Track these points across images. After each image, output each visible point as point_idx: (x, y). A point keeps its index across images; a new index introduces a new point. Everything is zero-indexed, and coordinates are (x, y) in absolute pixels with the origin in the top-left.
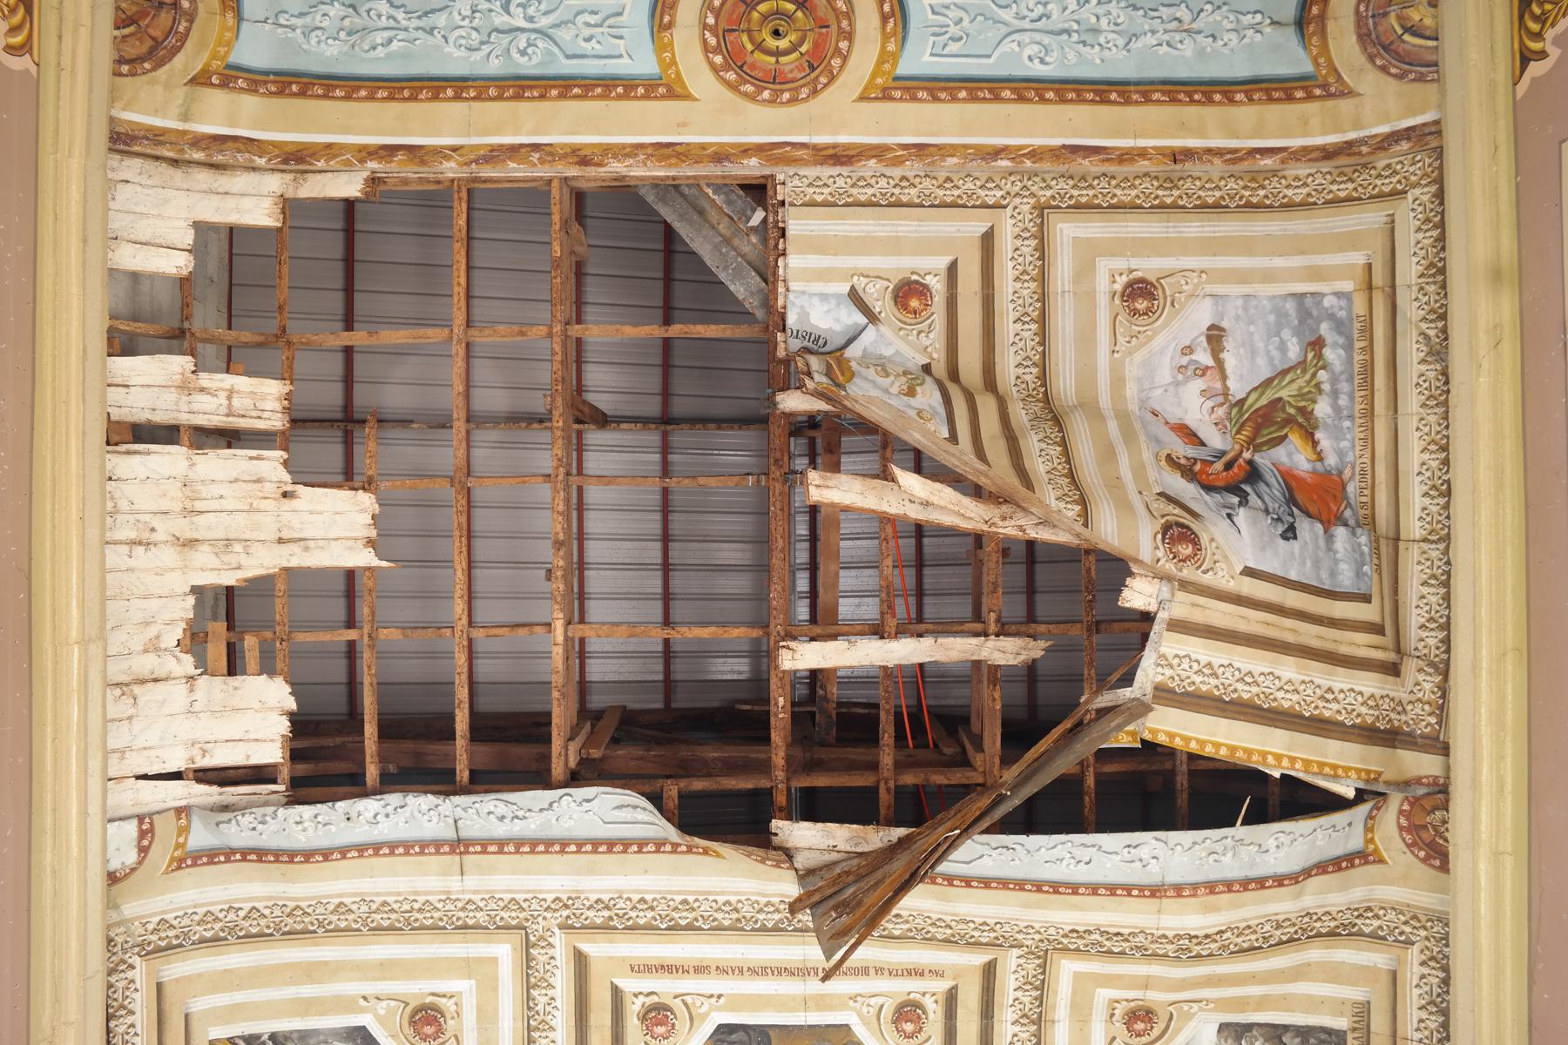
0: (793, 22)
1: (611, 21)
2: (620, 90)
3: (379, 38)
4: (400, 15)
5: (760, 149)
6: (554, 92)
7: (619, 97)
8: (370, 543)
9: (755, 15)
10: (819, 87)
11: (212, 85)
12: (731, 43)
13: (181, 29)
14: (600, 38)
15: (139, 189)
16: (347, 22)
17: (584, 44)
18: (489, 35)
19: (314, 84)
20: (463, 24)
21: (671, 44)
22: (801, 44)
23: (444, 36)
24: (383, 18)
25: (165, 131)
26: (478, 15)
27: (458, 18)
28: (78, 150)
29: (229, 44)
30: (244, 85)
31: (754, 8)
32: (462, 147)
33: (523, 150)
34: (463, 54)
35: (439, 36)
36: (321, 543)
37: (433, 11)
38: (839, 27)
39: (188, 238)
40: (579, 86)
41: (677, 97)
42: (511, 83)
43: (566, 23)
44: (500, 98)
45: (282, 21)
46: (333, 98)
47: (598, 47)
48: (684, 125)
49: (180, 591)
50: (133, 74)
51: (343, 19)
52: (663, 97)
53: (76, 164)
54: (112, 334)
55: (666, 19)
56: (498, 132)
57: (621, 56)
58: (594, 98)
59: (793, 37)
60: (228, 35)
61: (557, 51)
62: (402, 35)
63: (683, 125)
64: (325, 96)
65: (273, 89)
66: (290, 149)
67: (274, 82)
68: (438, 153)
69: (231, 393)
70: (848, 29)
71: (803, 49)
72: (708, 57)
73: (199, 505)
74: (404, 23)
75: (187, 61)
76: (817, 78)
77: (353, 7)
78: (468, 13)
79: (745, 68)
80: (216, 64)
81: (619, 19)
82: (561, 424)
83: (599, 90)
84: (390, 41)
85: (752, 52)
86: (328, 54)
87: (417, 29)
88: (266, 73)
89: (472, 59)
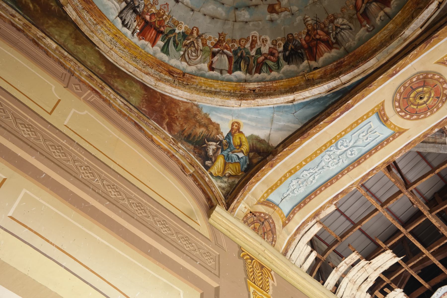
0: (424, 92)
1: (370, 130)
2: (385, 143)
3: (311, 179)
4: (311, 171)
5: (436, 126)
6: (368, 156)
7: (386, 144)
8: (395, 257)
9: (411, 99)
10: (444, 101)
11: (287, 223)
12: (409, 110)
13: (271, 221)
14: (370, 136)
15: (294, 253)
16: (299, 182)
17: (367, 141)
18: (339, 157)
19: (306, 200)
20: (329, 160)
21: (391, 123)
22: (431, 94)
23: (327, 167)
24: (308, 175)
25: (289, 241)
26: (332, 156)
27: (327, 160)
28: (288, 270)
29: (282, 213)
30: (292, 215)
31: (409, 97)
32: (354, 183)
33: (371, 172)
34: (335, 167)
35: (326, 167)
36: (384, 264)
37: (319, 164)
38: (440, 82)
39: (309, 248)
40: (373, 150)
41: (403, 132)
42: (354, 163)
43: (357, 140)
44: (354, 167)
45: (285, 196)
46: (312, 199)
47: (371, 138)
48: (410, 136)
49: (365, 295)
50: (275, 242)
51: (298, 182)
52: (399, 136)
53: (290, 272)
54: (317, 278)
55: (385, 119)
56: (360, 173)
57: (379, 136)
58: (379, 149)
59: (427, 95)
60: (280, 212)
61: (360, 147)
62: (316, 174)
63: (409, 137)
64: (310, 200)
65: (298, 209)
66: (313, 215)
67: (296, 208)
68: (348, 188)
69: (345, 263)
70: (443, 81)
71: (432, 95)
72: (405, 118)
73: (355, 281)
74: (314, 171)
75: (278, 225)
76: (442, 99)
77: (297, 178)
78: (329, 157)
79: (418, 112)
80: (284, 219)
81: (371, 129)
82: (422, 208)
83: (380, 147)
84: (314, 177)
85: (417, 108)
86: (302, 192)
87: (319, 170)
88: (293, 208)
89: (339, 165)
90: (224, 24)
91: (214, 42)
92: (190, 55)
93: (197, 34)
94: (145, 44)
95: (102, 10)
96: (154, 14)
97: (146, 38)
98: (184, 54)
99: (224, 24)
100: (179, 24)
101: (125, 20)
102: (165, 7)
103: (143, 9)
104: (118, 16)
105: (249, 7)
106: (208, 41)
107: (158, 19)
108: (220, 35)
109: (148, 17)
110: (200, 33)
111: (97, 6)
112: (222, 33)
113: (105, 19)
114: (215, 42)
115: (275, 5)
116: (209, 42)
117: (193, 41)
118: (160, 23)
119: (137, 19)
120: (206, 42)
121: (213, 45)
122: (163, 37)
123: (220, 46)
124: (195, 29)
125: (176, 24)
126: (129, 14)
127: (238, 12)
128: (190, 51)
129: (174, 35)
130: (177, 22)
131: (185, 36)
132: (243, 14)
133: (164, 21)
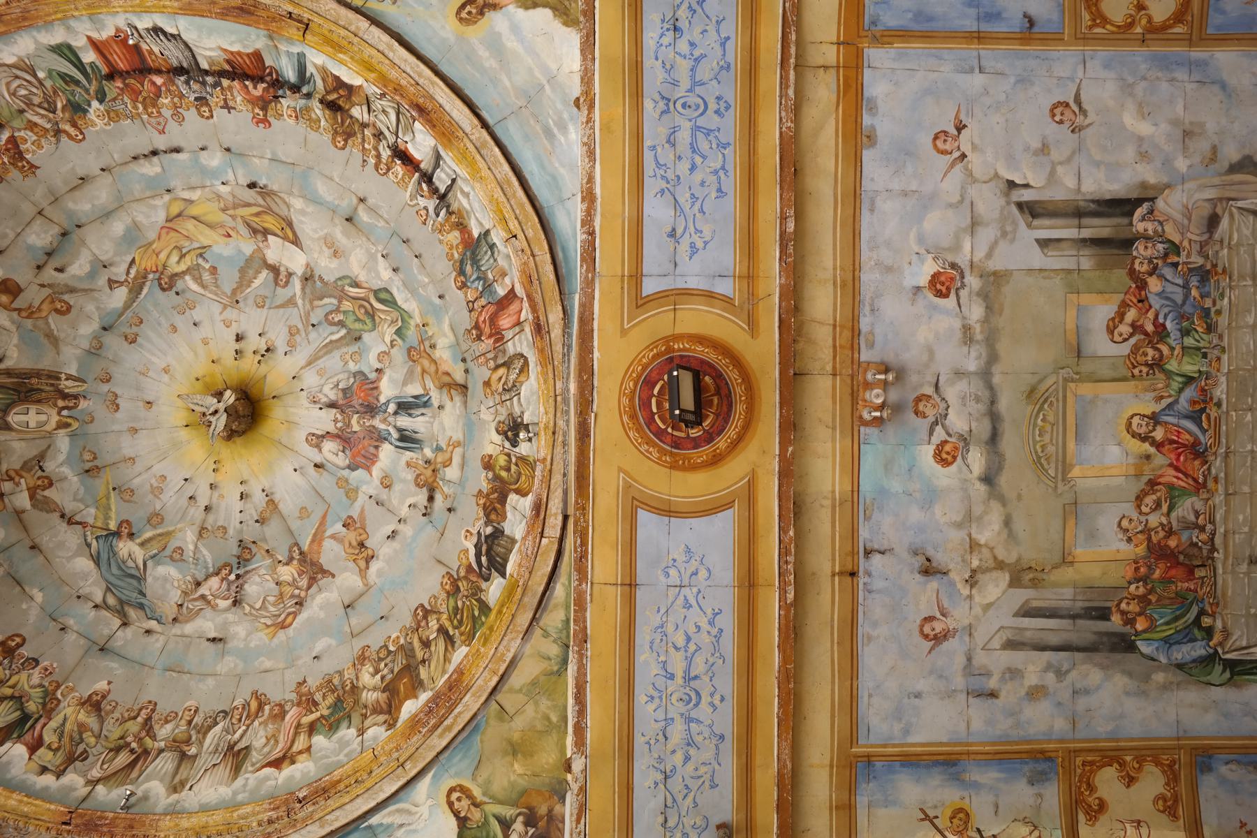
90: (51, 191)
91: (25, 146)
92: (25, 83)
93: (65, 132)
94: (103, 30)
95: (205, 21)
96: (159, 96)
97: (116, 41)
98: (35, 76)
99: (51, 191)
100: (109, 117)
101: (169, 40)
102: (159, 124)
103: (178, 87)
104: (179, 35)
105: (49, 254)
106: (35, 138)
107: (144, 94)
108: (32, 166)
109: (159, 80)
110: (64, 139)
111: (211, 17)
112: (34, 173)
113: (181, 9)
114: (22, 147)
115: (12, 299)
116: (30, 137)
117: (54, 112)
118: (134, 91)
119: (165, 60)
120: (36, 134)
121: (19, 141)
122: (100, 71)
123: (8, 150)
124: (80, 137)
125: (112, 115)
126: (181, 57)
127: (56, 230)
128: (35, 90)
129: (92, 92)
130: (116, 119)
131: (77, 109)
132: (43, 236)
133: (135, 101)
